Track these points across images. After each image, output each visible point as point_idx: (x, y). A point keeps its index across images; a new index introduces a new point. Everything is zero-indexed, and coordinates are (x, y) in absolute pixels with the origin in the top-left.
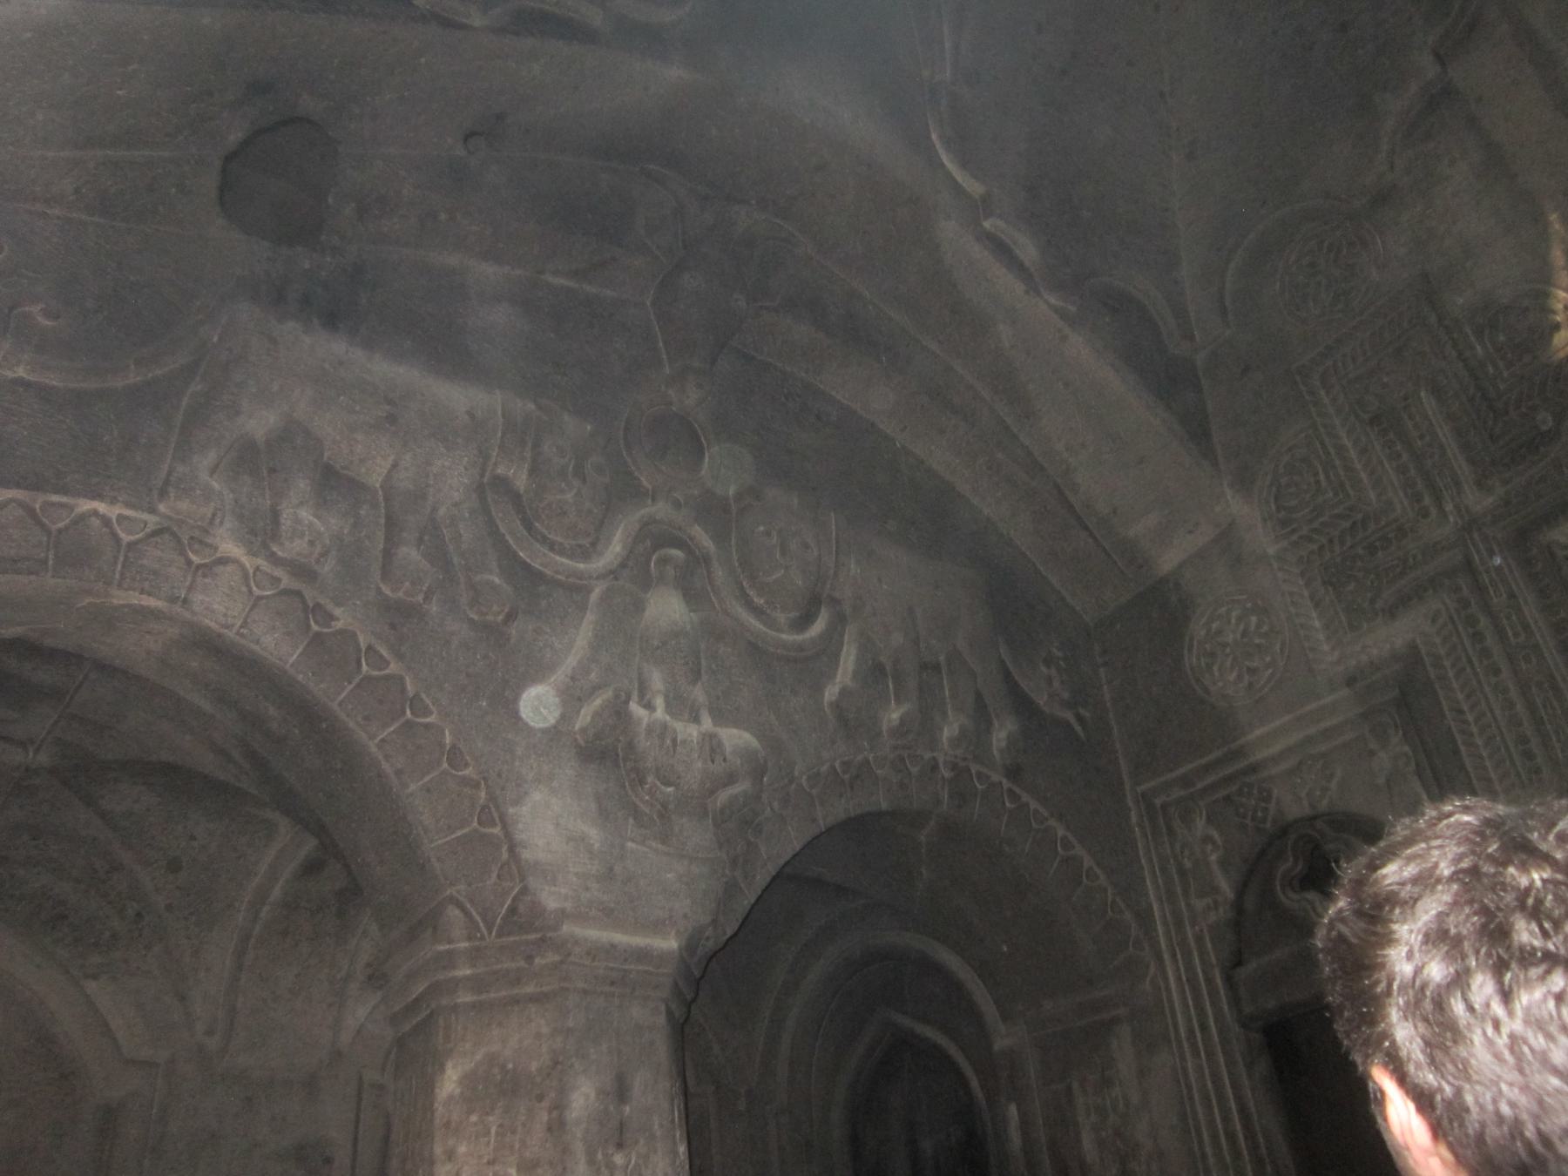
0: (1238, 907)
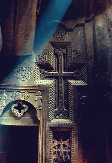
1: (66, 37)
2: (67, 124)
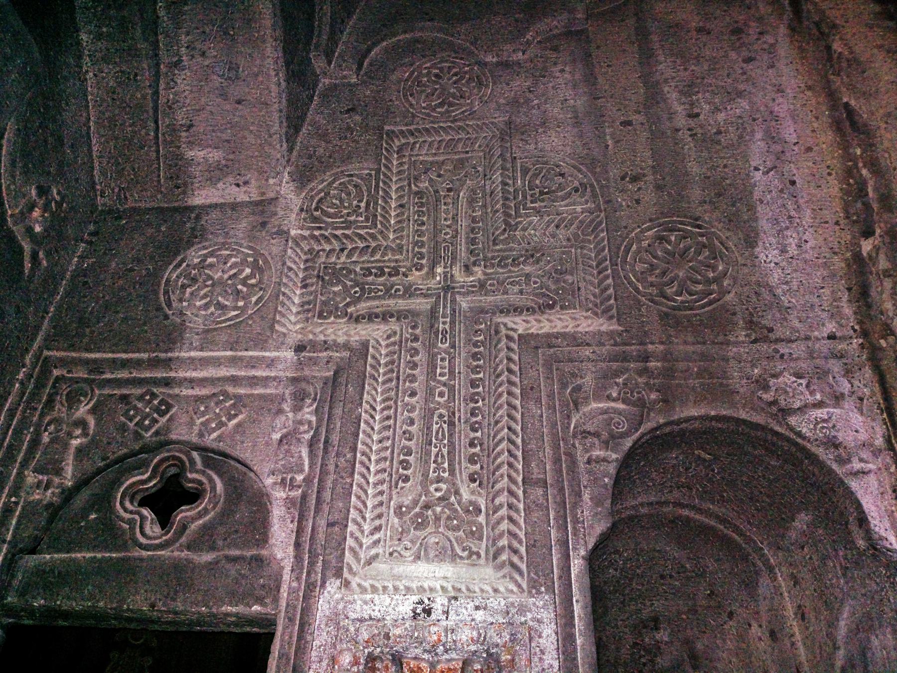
0: (68, 495)
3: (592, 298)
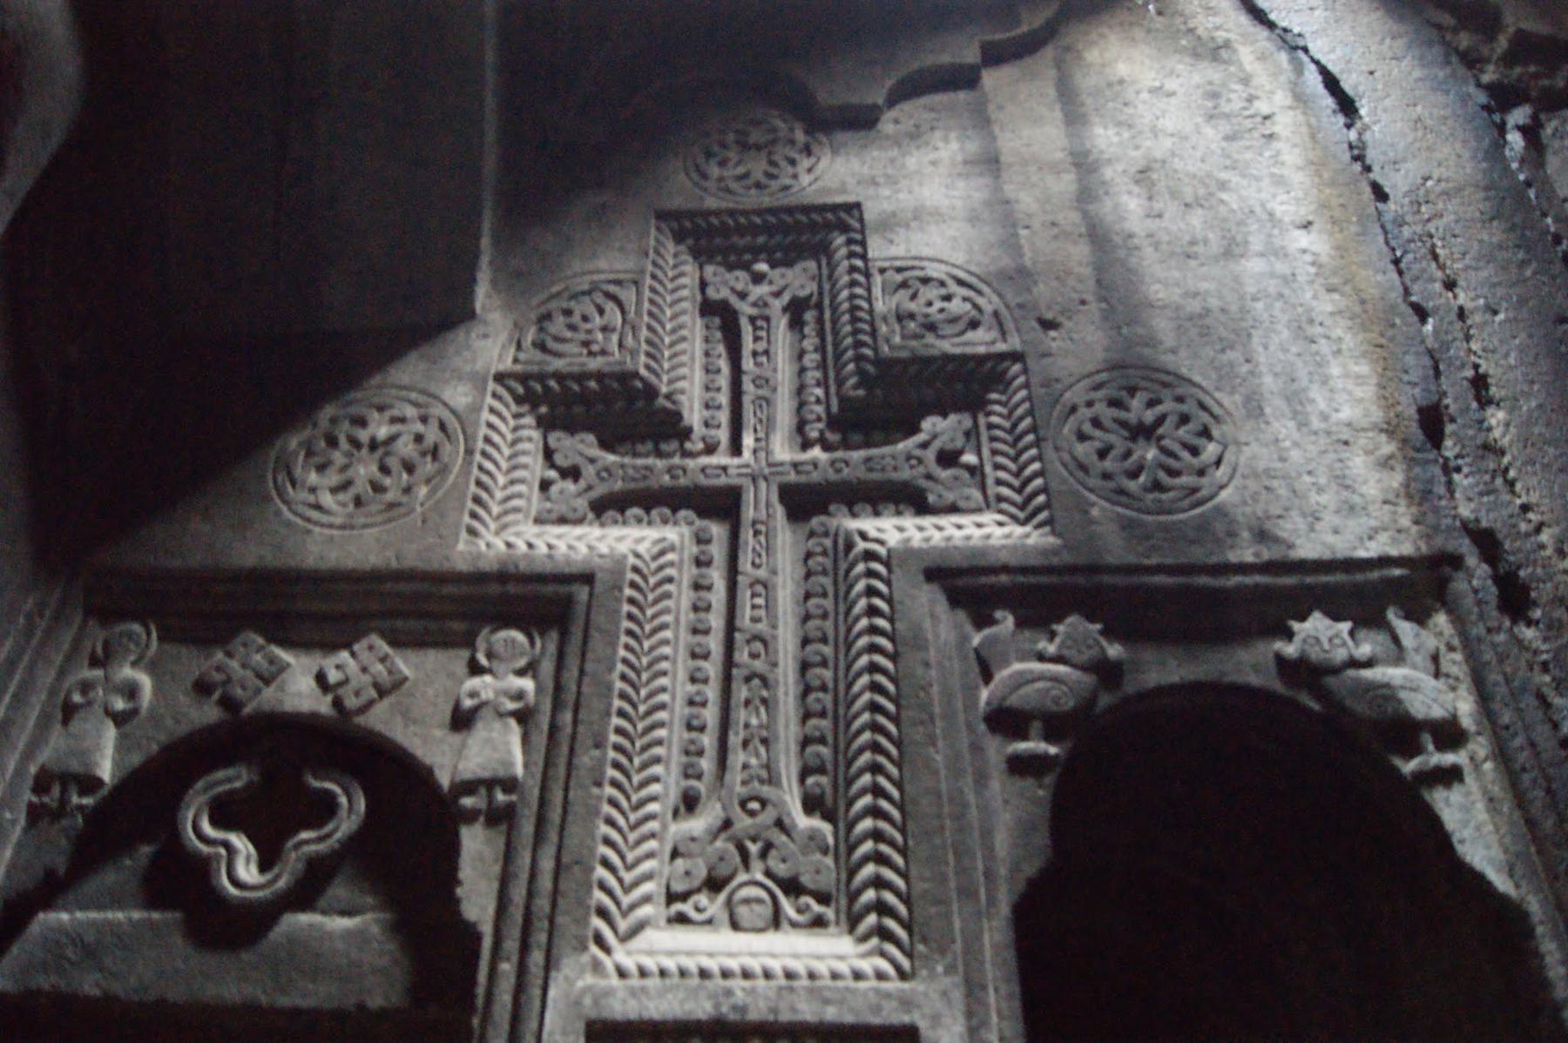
1: (810, 170)
2: (829, 982)
3: (1005, 491)
